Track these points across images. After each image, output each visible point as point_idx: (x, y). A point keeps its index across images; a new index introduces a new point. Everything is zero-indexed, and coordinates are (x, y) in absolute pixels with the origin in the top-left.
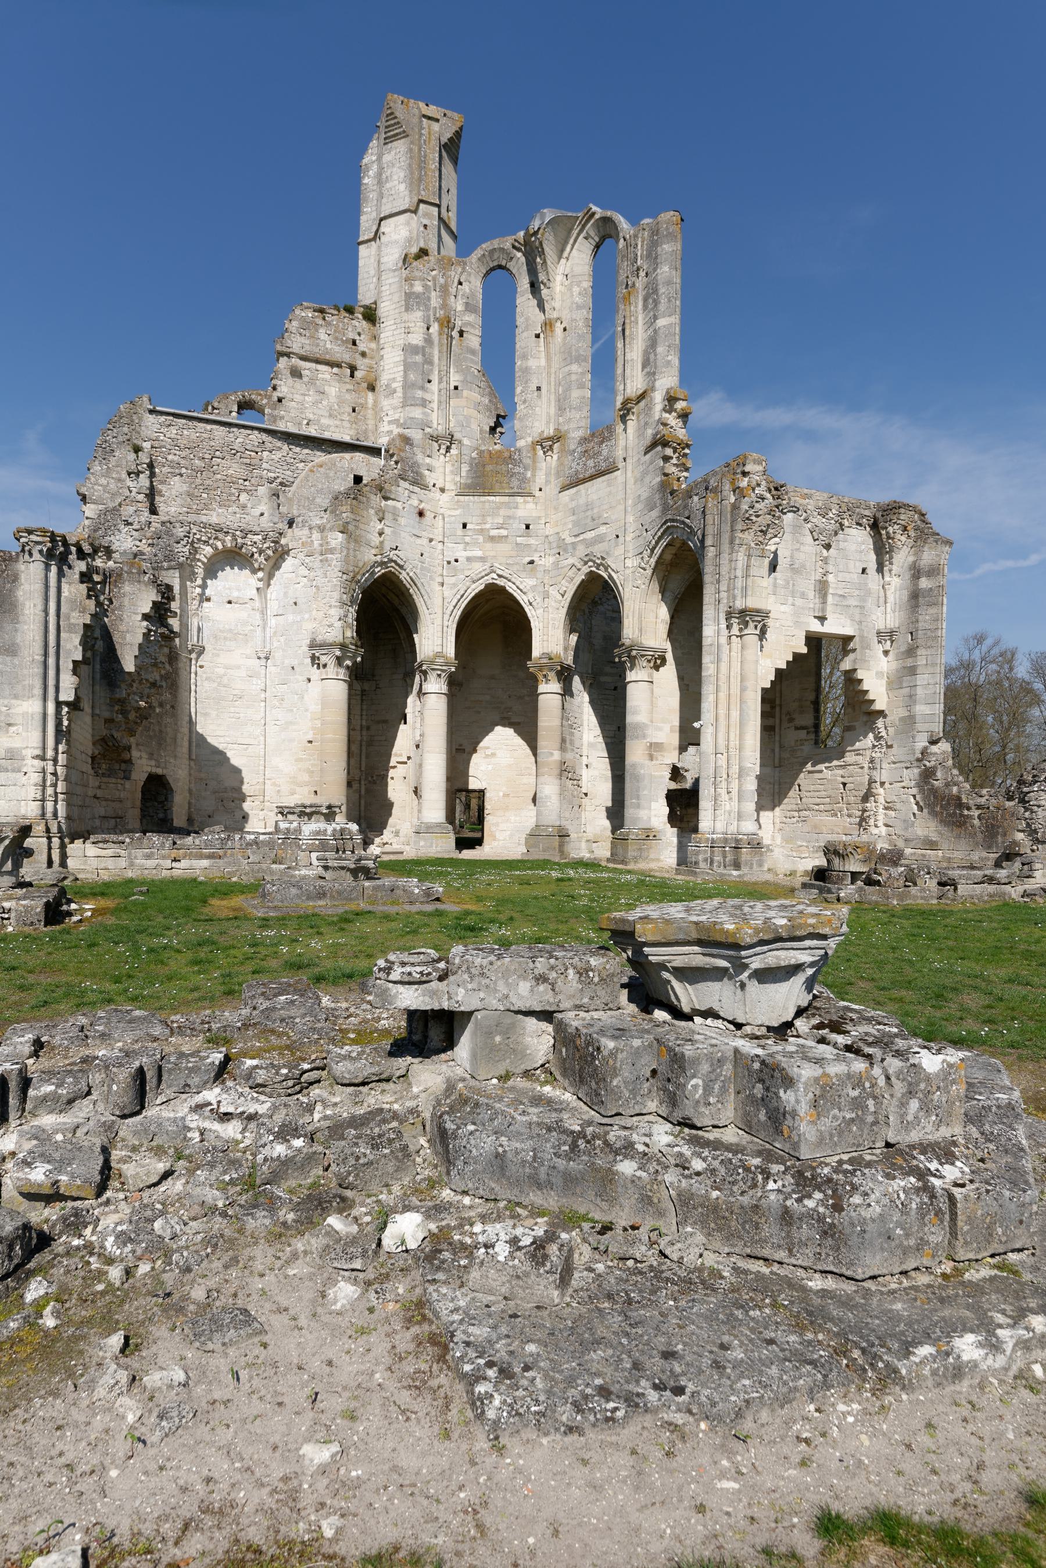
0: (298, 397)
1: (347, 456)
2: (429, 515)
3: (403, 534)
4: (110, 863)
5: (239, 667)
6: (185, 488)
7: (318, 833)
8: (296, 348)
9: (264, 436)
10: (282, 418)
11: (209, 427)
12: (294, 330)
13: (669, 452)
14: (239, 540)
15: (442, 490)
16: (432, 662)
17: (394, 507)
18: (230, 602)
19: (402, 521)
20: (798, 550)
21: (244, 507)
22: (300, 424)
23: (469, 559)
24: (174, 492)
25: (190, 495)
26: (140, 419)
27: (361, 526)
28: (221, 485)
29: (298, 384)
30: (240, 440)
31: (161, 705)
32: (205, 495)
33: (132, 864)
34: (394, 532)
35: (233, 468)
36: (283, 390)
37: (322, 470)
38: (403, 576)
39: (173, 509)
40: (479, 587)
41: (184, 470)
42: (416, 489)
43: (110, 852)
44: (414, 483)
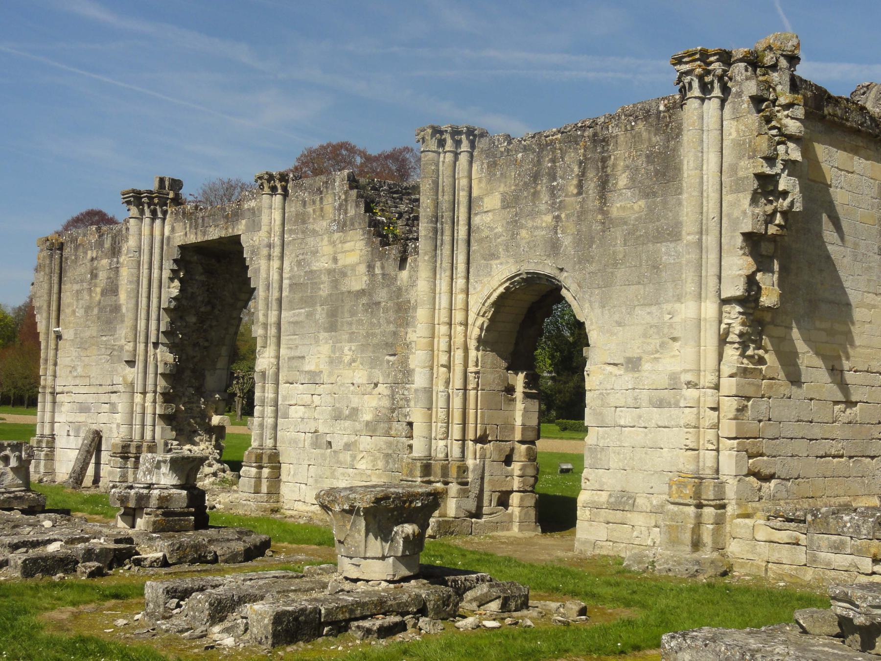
4: (784, 554)
33: (813, 561)
43: (783, 536)
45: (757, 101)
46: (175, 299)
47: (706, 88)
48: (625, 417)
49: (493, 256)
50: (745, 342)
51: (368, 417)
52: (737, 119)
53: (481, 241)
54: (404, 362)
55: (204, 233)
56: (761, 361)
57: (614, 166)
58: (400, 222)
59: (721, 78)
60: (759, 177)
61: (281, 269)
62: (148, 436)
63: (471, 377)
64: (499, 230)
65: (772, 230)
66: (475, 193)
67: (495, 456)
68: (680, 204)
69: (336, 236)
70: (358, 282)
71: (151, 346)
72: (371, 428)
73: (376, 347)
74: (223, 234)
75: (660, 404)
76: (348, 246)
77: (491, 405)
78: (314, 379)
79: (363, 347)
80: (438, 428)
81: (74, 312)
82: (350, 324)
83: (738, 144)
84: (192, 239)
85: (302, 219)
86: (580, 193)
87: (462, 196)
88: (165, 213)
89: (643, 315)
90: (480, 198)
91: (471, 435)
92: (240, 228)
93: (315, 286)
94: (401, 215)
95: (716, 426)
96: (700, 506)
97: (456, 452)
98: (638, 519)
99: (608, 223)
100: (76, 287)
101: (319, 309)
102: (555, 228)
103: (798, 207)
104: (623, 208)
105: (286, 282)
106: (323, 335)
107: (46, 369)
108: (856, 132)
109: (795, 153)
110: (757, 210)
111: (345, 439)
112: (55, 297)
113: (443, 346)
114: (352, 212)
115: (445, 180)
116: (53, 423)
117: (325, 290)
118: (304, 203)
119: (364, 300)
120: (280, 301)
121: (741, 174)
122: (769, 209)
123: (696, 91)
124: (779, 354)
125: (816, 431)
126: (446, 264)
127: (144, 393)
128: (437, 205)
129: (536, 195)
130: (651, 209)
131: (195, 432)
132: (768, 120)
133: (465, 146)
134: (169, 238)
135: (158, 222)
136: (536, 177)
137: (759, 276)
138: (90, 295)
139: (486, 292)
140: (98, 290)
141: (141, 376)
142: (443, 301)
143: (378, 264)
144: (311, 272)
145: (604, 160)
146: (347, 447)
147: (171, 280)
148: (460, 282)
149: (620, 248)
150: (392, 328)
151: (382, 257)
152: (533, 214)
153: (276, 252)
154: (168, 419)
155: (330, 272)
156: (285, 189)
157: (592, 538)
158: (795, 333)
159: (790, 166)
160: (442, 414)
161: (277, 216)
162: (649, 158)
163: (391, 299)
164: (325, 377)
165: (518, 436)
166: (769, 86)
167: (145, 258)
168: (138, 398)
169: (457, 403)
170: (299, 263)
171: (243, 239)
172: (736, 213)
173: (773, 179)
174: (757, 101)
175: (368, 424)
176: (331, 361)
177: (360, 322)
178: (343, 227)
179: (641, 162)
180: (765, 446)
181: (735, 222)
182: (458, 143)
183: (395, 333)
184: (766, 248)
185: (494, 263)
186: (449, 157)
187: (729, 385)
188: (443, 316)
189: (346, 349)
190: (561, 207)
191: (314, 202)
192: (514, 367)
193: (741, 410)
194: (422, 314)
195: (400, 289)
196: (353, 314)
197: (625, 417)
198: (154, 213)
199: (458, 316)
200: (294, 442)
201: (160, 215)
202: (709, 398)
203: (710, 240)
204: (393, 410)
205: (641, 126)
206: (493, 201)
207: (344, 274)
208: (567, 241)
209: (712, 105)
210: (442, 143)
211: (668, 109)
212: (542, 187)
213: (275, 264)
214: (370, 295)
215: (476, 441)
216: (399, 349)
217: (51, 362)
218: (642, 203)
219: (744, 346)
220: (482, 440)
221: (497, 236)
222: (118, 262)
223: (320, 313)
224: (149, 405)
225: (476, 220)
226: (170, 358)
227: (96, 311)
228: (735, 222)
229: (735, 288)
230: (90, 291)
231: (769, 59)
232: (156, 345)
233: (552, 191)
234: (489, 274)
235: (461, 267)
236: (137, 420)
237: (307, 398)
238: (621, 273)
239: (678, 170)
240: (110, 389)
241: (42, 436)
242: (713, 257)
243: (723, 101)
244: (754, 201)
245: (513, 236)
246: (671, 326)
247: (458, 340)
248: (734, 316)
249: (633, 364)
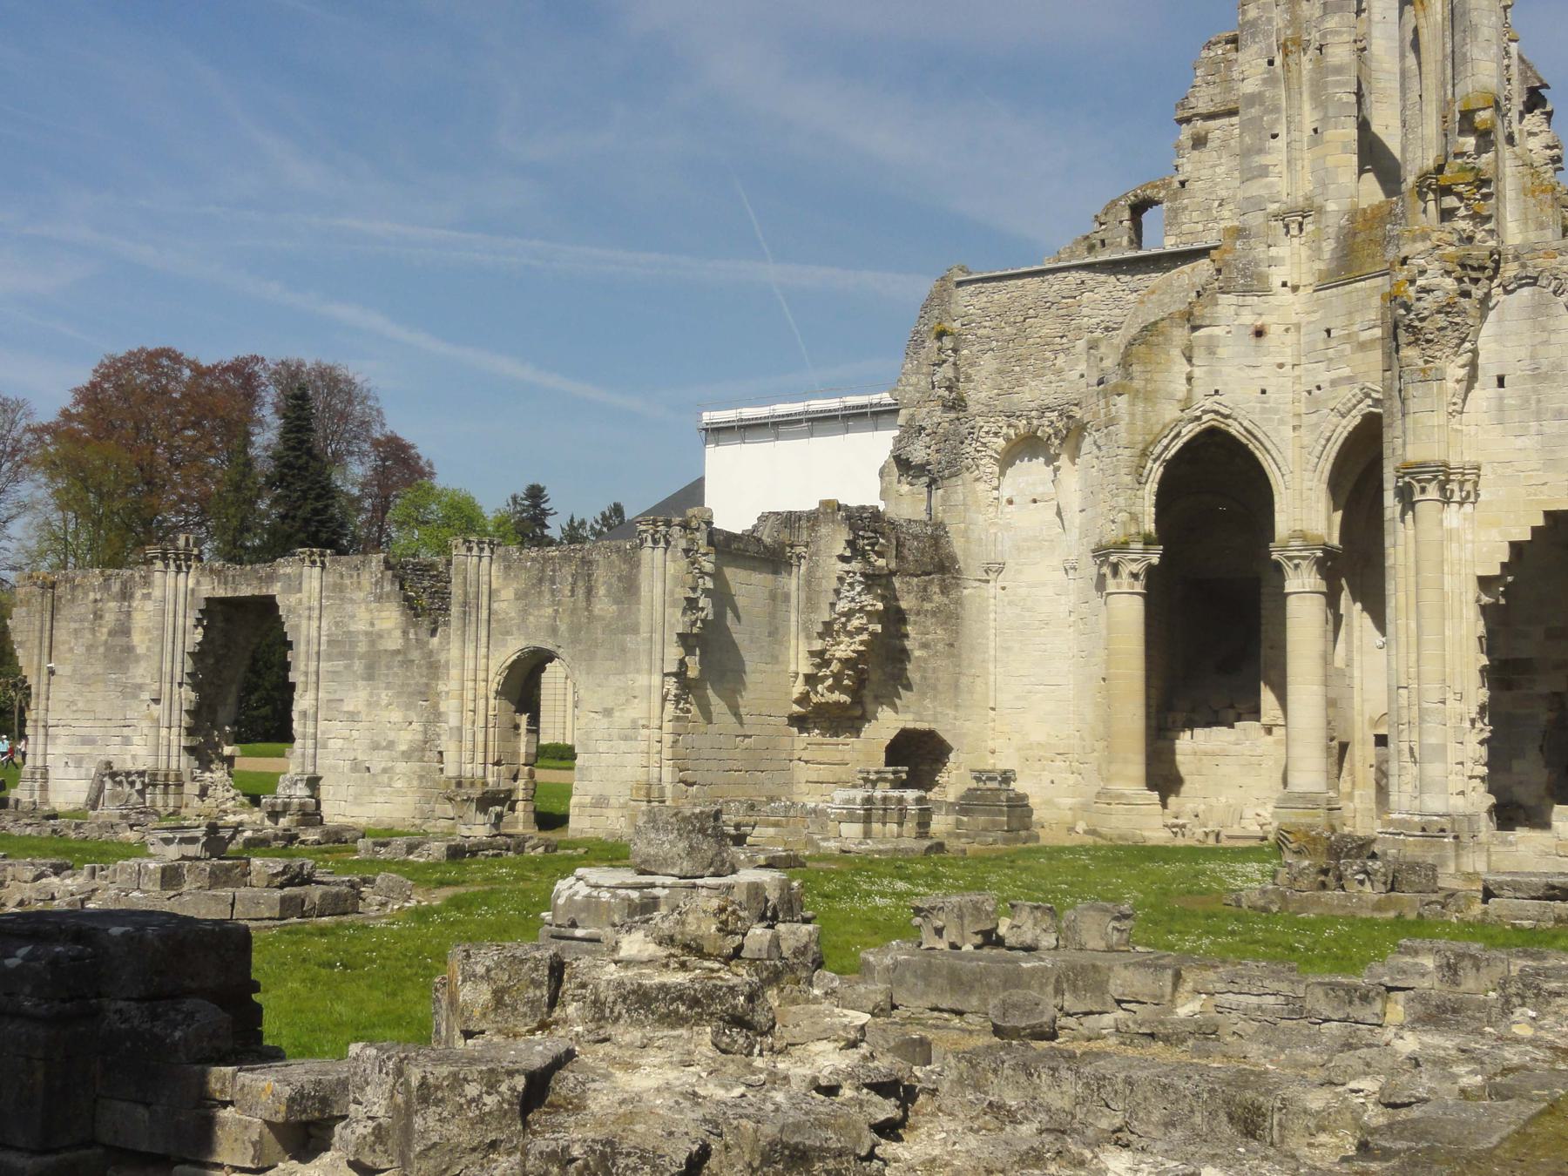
0: (1205, 173)
1: (1187, 268)
2: (1274, 332)
3: (1226, 370)
5: (1044, 584)
6: (995, 365)
7: (848, 801)
8: (1203, 106)
9: (1084, 275)
10: (1186, 208)
11: (1020, 282)
12: (1198, 81)
13: (1450, 202)
14: (1035, 422)
15: (1295, 289)
16: (1285, 548)
17: (1210, 337)
18: (1035, 501)
19: (1222, 352)
20: (1546, 343)
21: (1060, 372)
22: (1209, 209)
23: (1334, 383)
24: (984, 373)
25: (1000, 372)
26: (950, 296)
27: (1156, 376)
28: (1033, 350)
29: (1207, 155)
30: (1056, 287)
31: (924, 646)
32: (1017, 369)
34: (1211, 373)
35: (1047, 327)
36: (1187, 169)
37: (1154, 297)
38: (1234, 429)
39: (984, 394)
40: (1354, 420)
41: (994, 343)
42: (1250, 300)
44: (1246, 291)
45: (686, 551)
46: (199, 644)
47: (655, 541)
48: (602, 746)
49: (508, 633)
50: (677, 700)
51: (404, 747)
52: (674, 561)
53: (498, 621)
54: (435, 706)
55: (235, 590)
56: (688, 711)
57: (596, 581)
58: (424, 596)
59: (665, 537)
60: (687, 599)
61: (319, 627)
62: (174, 765)
63: (490, 718)
64: (513, 614)
65: (695, 630)
66: (494, 586)
67: (507, 775)
68: (639, 610)
69: (373, 605)
70: (394, 642)
71: (176, 686)
72: (407, 756)
73: (411, 695)
74: (256, 593)
75: (626, 738)
76: (384, 614)
77: (504, 739)
78: (353, 717)
79: (399, 694)
80: (467, 756)
81: (71, 650)
82: (387, 675)
83: (675, 578)
84: (221, 593)
85: (339, 588)
86: (572, 596)
87: (485, 588)
88: (189, 567)
89: (615, 681)
90: (498, 591)
91: (490, 760)
92: (275, 589)
93: (353, 644)
94: (425, 589)
95: (660, 752)
96: (649, 802)
97: (480, 772)
98: (611, 813)
99: (591, 618)
100: (73, 625)
101: (357, 662)
102: (555, 618)
103: (710, 617)
104: (602, 609)
105: (324, 639)
106: (361, 683)
107: (38, 704)
108: (754, 558)
109: (710, 584)
110: (686, 619)
111: (383, 765)
112: (47, 634)
113: (471, 696)
114: (387, 588)
115: (471, 575)
116: (45, 755)
117: (362, 647)
118: (342, 576)
119: (400, 658)
120: (318, 653)
121: (676, 596)
122: (693, 617)
123: (650, 543)
124: (700, 706)
125: (724, 755)
126: (473, 637)
127: (170, 728)
128: (466, 594)
129: (540, 593)
130: (620, 612)
131: (212, 762)
132: (693, 564)
133: (487, 552)
134: (193, 590)
135: (182, 575)
136: (541, 581)
137: (687, 659)
138: (94, 635)
139: (503, 659)
140: (105, 630)
141: (167, 712)
142: (470, 664)
143: (412, 631)
144: (349, 632)
145: (590, 576)
146: (385, 771)
147: (196, 627)
148: (483, 651)
149: (600, 635)
150: (424, 680)
151: (415, 625)
152: (539, 606)
153: (316, 614)
154: (190, 750)
155: (367, 633)
156: (323, 563)
157: (580, 827)
158: (710, 692)
159: (707, 592)
160: (469, 746)
161: (316, 584)
162: (620, 579)
163: (424, 658)
164: (363, 716)
165: (522, 761)
166: (693, 541)
167: (171, 607)
168: (164, 732)
169: (480, 737)
170: (337, 624)
171: (278, 599)
172: (673, 621)
173: (696, 600)
174: (686, 551)
175: (403, 752)
176: (369, 704)
177: (396, 674)
178: (379, 598)
179: (614, 580)
180: (690, 764)
181: (672, 626)
182: (482, 550)
183: (427, 685)
184: (691, 641)
185: (509, 638)
186: (475, 560)
187: (668, 726)
188: (469, 674)
189: (383, 696)
190: (559, 603)
191: (351, 576)
192: (520, 710)
193: (675, 742)
194: (454, 672)
195: (431, 651)
196: (389, 667)
197: (602, 746)
198: (179, 569)
199: (481, 675)
200: (334, 768)
201: (184, 569)
202: (656, 734)
203: (657, 637)
204: (426, 743)
205: (614, 557)
206: (508, 593)
207: (380, 636)
208: (563, 627)
209: (659, 552)
210: (470, 549)
211: (632, 548)
212: (546, 587)
213: (315, 624)
214: (405, 654)
215: (494, 764)
216: (431, 697)
217: (43, 696)
218: (615, 607)
219: (677, 702)
220: (498, 763)
221: (512, 619)
222: (130, 606)
223: (358, 666)
224: (174, 738)
225: (495, 606)
226: (193, 696)
227: (101, 650)
228: (672, 626)
229: (672, 667)
230: (93, 631)
231: (694, 524)
232: (180, 685)
233: (553, 592)
234: (505, 646)
235: (484, 639)
236: (163, 751)
237: (346, 733)
238: (600, 652)
239: (638, 589)
240: (123, 723)
241: (35, 767)
242: (658, 648)
243: (666, 549)
244: (684, 613)
245: (524, 620)
246: (633, 689)
247: (482, 692)
248: (672, 685)
249: (608, 712)
